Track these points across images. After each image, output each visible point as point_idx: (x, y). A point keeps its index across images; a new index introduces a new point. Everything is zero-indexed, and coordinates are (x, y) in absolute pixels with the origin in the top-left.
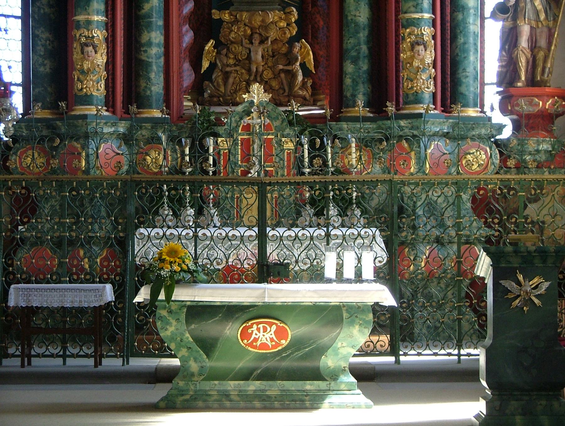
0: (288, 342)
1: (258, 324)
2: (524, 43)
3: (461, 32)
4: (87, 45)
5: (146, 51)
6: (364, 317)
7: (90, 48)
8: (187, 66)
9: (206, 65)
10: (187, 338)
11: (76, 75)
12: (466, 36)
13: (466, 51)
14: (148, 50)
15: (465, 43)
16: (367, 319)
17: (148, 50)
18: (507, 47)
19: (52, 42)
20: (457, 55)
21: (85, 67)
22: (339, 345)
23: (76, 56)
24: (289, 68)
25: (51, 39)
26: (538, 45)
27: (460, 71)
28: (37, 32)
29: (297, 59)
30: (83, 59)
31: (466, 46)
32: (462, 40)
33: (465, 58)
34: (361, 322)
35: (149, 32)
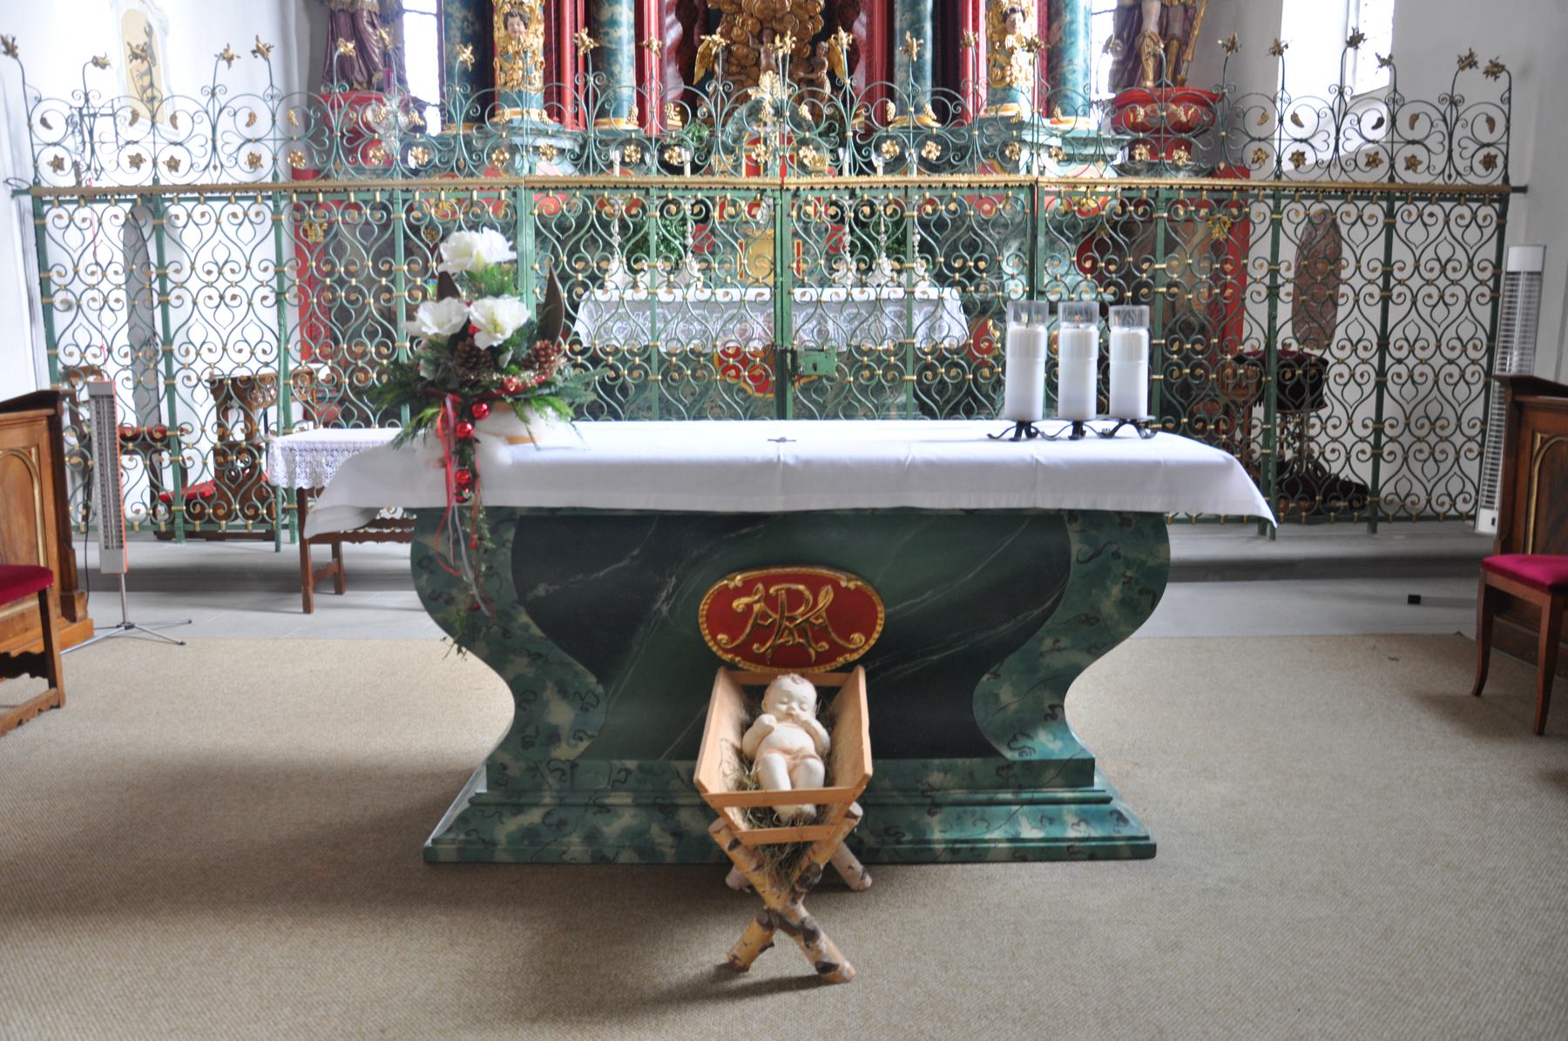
0: (872, 642)
1: (768, 582)
2: (1151, 26)
3: (1066, 6)
4: (510, 14)
5: (607, 34)
6: (1143, 557)
7: (517, 19)
8: (672, 70)
9: (699, 72)
10: (526, 628)
11: (497, 62)
12: (1072, 11)
13: (1073, 34)
14: (611, 31)
15: (1072, 22)
16: (1151, 563)
17: (611, 31)
18: (1125, 35)
19: (473, 24)
20: (1061, 39)
21: (511, 50)
22: (1048, 643)
23: (499, 34)
24: (813, 76)
25: (470, 19)
26: (1170, 32)
27: (1066, 62)
28: (449, 10)
29: (824, 64)
30: (509, 38)
31: (1074, 26)
32: (1068, 18)
33: (1072, 43)
34: (1129, 573)
35: (611, 5)
